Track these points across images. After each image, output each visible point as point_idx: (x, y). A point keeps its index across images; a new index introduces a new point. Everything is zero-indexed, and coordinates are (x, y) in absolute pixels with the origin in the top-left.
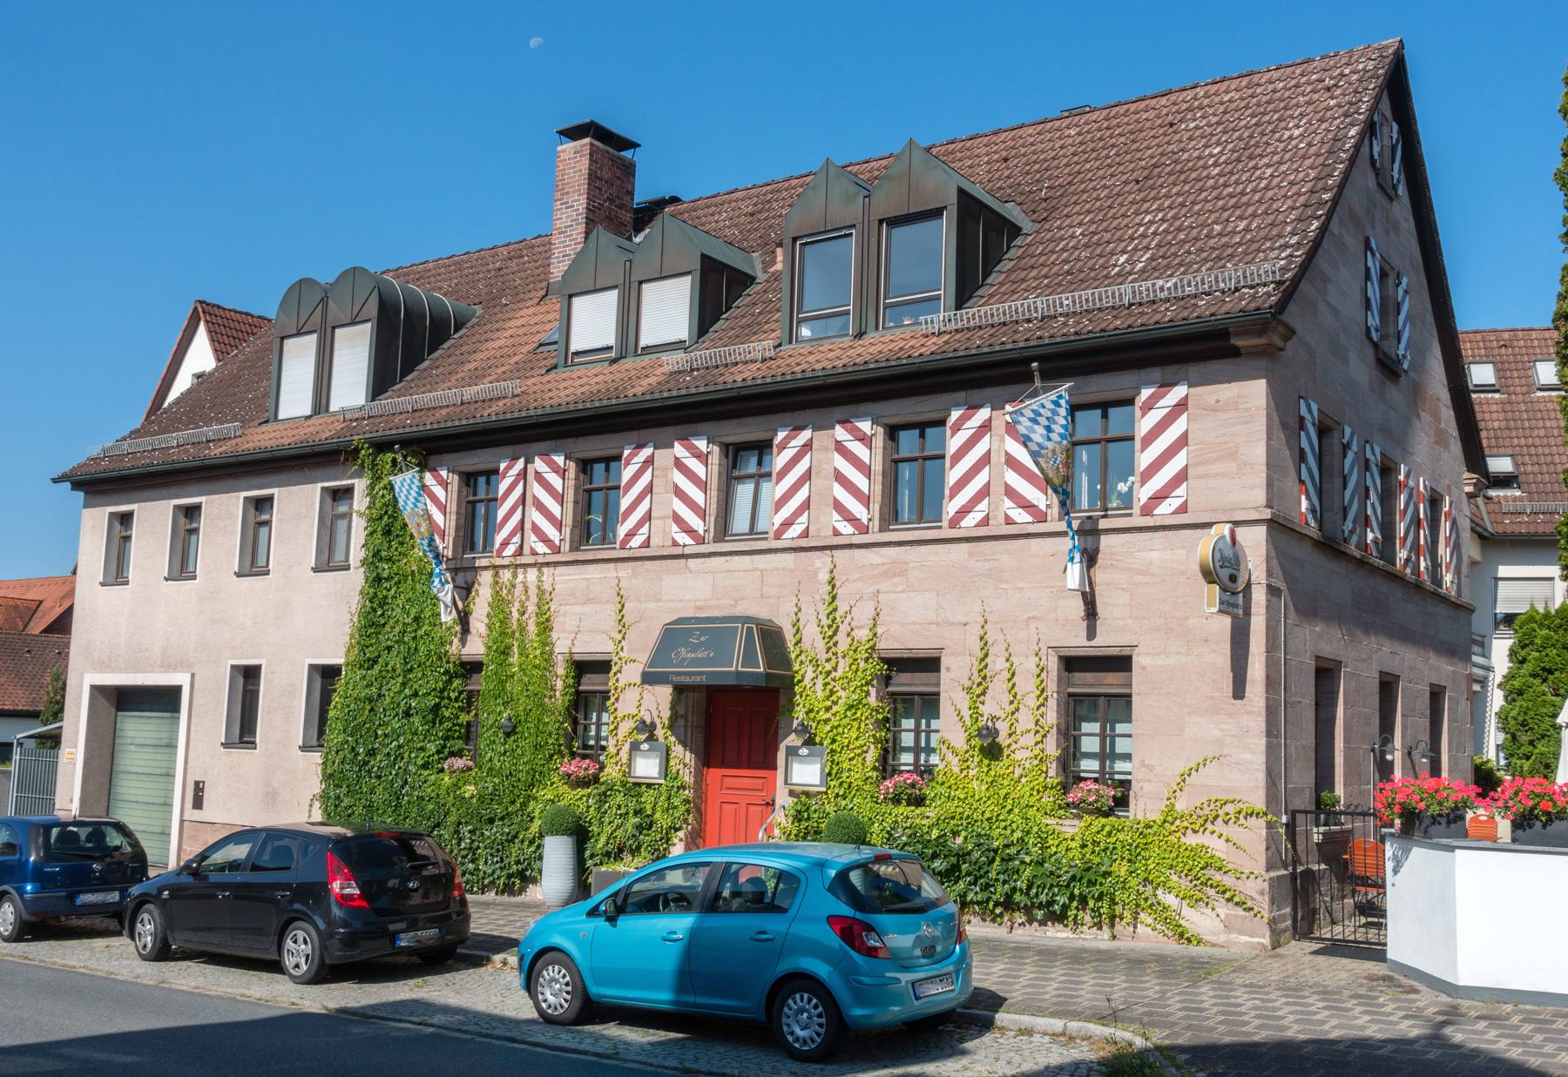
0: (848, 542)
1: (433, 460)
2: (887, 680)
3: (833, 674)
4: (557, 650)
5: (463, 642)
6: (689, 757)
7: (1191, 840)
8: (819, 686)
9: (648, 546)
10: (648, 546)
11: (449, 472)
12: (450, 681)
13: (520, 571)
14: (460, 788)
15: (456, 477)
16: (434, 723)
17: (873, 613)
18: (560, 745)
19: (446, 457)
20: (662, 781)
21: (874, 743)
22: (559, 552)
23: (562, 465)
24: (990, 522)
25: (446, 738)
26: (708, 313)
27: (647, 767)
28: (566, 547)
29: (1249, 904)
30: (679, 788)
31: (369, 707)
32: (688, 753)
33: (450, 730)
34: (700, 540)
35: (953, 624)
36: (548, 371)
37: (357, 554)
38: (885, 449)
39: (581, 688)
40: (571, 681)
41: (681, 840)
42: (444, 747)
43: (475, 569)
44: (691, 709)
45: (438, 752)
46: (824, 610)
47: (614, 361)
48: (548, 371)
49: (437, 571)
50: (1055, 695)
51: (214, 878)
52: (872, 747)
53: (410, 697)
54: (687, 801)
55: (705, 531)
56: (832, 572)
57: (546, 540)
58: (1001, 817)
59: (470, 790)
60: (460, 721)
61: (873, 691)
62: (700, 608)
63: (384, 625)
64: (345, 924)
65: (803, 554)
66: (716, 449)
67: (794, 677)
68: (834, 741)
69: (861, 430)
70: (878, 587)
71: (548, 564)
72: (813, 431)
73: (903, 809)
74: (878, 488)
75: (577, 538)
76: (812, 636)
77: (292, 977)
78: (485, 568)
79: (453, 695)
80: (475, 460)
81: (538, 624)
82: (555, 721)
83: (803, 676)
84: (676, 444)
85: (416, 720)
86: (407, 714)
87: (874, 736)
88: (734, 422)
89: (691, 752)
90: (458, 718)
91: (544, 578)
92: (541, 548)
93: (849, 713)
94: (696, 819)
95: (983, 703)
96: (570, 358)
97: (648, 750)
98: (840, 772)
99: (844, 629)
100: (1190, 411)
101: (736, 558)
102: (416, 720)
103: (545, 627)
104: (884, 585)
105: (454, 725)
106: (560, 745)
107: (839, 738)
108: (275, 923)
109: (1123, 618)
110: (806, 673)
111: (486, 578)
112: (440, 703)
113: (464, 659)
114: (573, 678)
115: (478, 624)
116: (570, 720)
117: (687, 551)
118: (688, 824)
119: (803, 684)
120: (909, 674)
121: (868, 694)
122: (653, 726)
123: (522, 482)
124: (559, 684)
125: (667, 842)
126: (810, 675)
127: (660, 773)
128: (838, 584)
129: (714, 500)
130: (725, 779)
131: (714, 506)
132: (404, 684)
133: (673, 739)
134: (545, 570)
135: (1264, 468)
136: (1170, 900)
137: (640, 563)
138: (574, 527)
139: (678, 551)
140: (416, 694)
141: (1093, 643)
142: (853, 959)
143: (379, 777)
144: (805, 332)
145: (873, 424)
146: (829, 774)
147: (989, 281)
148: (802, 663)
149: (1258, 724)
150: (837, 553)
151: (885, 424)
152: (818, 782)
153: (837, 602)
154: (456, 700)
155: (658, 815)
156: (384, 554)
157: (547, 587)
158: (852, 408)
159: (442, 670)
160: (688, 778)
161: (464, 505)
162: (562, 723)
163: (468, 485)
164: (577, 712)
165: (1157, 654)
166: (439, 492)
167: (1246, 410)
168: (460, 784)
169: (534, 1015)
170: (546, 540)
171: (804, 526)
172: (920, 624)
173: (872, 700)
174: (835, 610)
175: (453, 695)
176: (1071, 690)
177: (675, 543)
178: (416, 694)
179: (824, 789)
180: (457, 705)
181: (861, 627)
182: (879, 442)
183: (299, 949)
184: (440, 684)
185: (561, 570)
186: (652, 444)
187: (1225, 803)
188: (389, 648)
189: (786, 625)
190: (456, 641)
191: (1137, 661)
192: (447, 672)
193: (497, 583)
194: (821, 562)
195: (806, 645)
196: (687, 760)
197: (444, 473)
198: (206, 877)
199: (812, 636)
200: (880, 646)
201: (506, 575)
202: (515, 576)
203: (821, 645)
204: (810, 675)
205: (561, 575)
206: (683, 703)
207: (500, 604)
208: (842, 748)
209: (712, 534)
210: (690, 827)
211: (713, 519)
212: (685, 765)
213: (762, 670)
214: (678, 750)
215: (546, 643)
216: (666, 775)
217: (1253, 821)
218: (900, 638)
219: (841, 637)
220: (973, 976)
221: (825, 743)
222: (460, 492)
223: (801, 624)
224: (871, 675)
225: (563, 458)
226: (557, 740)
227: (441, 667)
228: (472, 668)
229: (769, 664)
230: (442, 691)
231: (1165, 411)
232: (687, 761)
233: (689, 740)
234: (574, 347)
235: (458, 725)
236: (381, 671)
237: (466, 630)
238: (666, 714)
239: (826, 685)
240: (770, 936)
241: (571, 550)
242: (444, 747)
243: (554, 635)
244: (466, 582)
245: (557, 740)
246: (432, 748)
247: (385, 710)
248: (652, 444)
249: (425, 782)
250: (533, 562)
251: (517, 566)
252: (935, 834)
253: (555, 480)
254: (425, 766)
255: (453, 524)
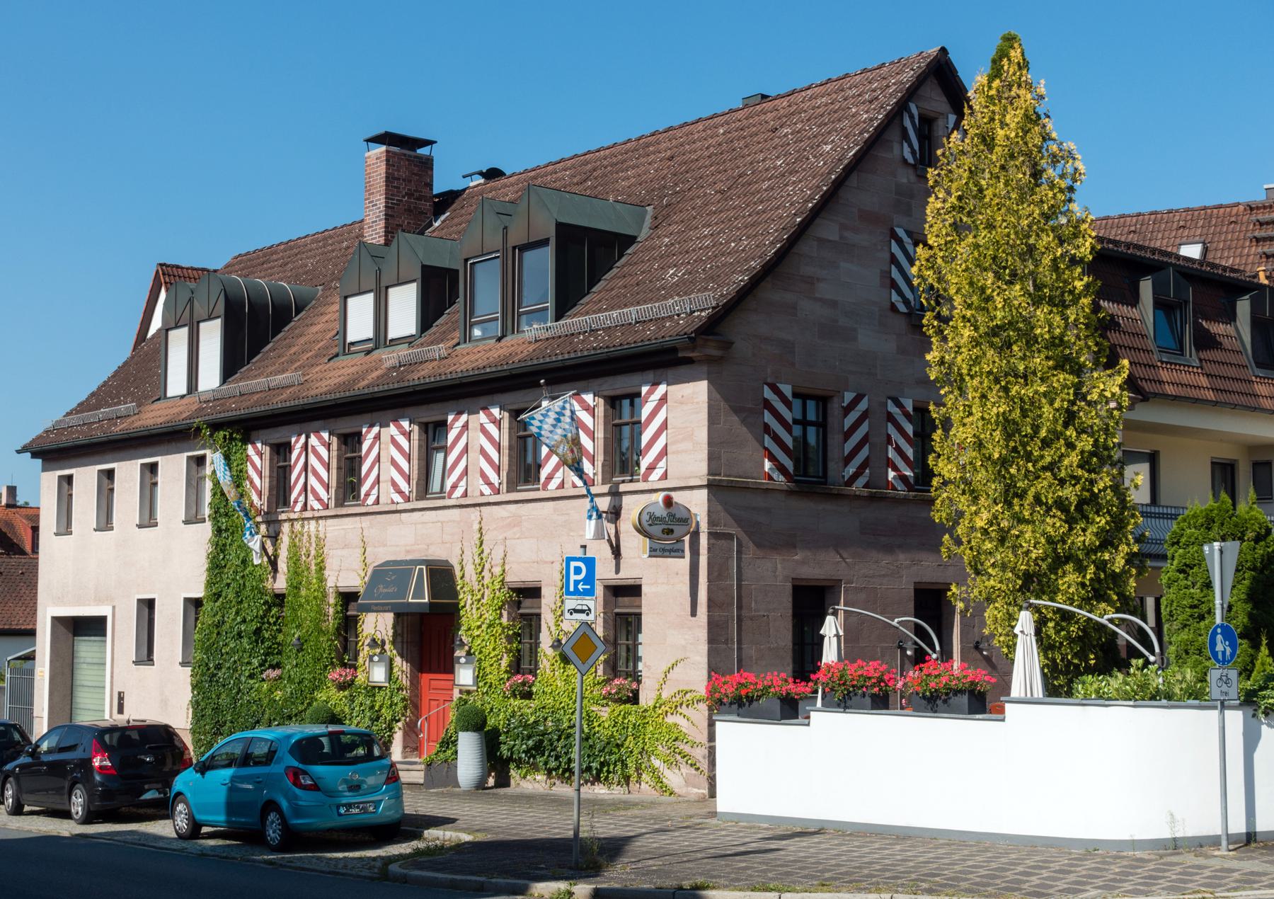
0: (486, 501)
1: (254, 434)
2: (519, 605)
3: (482, 601)
4: (329, 585)
5: (274, 578)
6: (406, 667)
7: (670, 720)
8: (474, 611)
9: (378, 504)
10: (378, 504)
11: (262, 444)
12: (269, 610)
13: (306, 522)
14: (273, 693)
15: (268, 448)
16: (258, 643)
17: (503, 555)
18: (332, 658)
19: (261, 432)
20: (387, 685)
21: (506, 653)
22: (328, 508)
23: (327, 440)
24: (565, 486)
25: (267, 654)
26: (429, 314)
27: (378, 674)
28: (332, 504)
29: (698, 765)
30: (398, 689)
31: (216, 631)
32: (404, 663)
33: (270, 647)
34: (408, 500)
35: (546, 562)
36: (329, 360)
37: (207, 511)
38: (605, 416)
39: (349, 613)
40: (339, 608)
41: (400, 729)
42: (265, 661)
43: (280, 522)
44: (405, 629)
45: (261, 665)
46: (476, 551)
47: (368, 352)
48: (329, 360)
49: (248, 525)
50: (602, 615)
51: (45, 759)
52: (505, 655)
53: (240, 623)
54: (404, 699)
55: (410, 492)
56: (480, 523)
57: (319, 500)
58: (570, 707)
59: (278, 695)
60: (278, 640)
61: (505, 613)
62: (408, 552)
63: (225, 566)
64: (102, 784)
65: (464, 510)
66: (416, 428)
67: (459, 603)
68: (481, 652)
69: (586, 402)
70: (505, 535)
71: (321, 518)
72: (469, 415)
73: (517, 702)
74: (506, 459)
75: (341, 496)
76: (470, 571)
77: (76, 820)
78: (285, 521)
79: (272, 620)
80: (278, 435)
81: (316, 565)
82: (326, 643)
83: (466, 602)
84: (391, 424)
85: (245, 640)
86: (240, 635)
87: (506, 648)
88: (424, 407)
89: (407, 662)
90: (276, 638)
91: (320, 529)
92: (317, 505)
93: (489, 630)
94: (412, 713)
95: (562, 621)
96: (347, 348)
97: (465, 663)
98: (485, 675)
99: (487, 566)
100: (668, 404)
101: (428, 513)
102: (245, 640)
103: (321, 569)
104: (509, 534)
105: (273, 644)
106: (332, 658)
107: (484, 650)
108: (67, 785)
109: (634, 558)
110: (465, 598)
111: (286, 528)
112: (261, 627)
113: (277, 592)
114: (341, 606)
115: (282, 565)
116: (341, 639)
117: (400, 507)
118: (406, 717)
119: (464, 609)
120: (530, 600)
121: (501, 615)
122: (383, 642)
123: (304, 453)
124: (331, 611)
125: (390, 731)
126: (469, 602)
127: (385, 679)
128: (484, 533)
129: (416, 467)
130: (432, 682)
131: (416, 472)
132: (237, 613)
133: (395, 652)
134: (320, 522)
135: (706, 446)
136: (656, 763)
137: (374, 516)
138: (338, 487)
139: (393, 508)
140: (244, 621)
141: (620, 576)
142: (294, 792)
143: (224, 686)
144: (477, 332)
145: (595, 396)
146: (478, 677)
147: (593, 290)
148: (464, 593)
149: (702, 634)
150: (483, 509)
151: (338, 434)
152: (471, 683)
153: (483, 546)
154: (275, 624)
155: (383, 710)
156: (222, 510)
157: (321, 535)
158: (489, 398)
159: (262, 602)
160: (405, 682)
161: (275, 470)
162: (333, 641)
163: (278, 453)
164: (347, 634)
165: (652, 584)
166: (256, 459)
167: (697, 403)
168: (273, 690)
169: (176, 836)
170: (319, 500)
171: (464, 488)
172: (529, 563)
173: (505, 621)
174: (482, 552)
175: (272, 620)
176: (617, 610)
177: (393, 502)
178: (244, 621)
179: (475, 688)
180: (275, 628)
181: (497, 565)
182: (600, 411)
183: (78, 804)
184: (261, 612)
185: (330, 521)
186: (378, 424)
187: (687, 693)
188: (228, 585)
189: (455, 562)
190: (271, 580)
191: (644, 589)
192: (266, 603)
193: (293, 532)
194: (474, 514)
195: (467, 579)
196: (404, 669)
197: (259, 445)
198: (39, 758)
199: (470, 571)
200: (507, 579)
201: (298, 526)
202: (303, 526)
203: (474, 577)
204: (469, 602)
205: (329, 526)
206: (400, 624)
207: (294, 546)
208: (485, 657)
209: (414, 494)
210: (408, 719)
211: (415, 482)
212: (403, 672)
213: (426, 600)
214: (398, 660)
215: (321, 580)
216: (390, 679)
217: (701, 704)
218: (519, 574)
219: (486, 573)
220: (405, 804)
221: (477, 653)
222: (271, 460)
223: (464, 563)
224: (502, 601)
225: (327, 434)
226: (330, 654)
227: (261, 599)
228: (280, 598)
229: (433, 594)
230: (262, 618)
231: (459, 429)
232: (404, 669)
233: (405, 652)
234: (350, 339)
235: (277, 643)
236: (223, 603)
237: (275, 569)
238: (391, 632)
239: (478, 609)
240: (261, 779)
241: (336, 506)
242: (265, 661)
243: (326, 573)
244: (275, 531)
245: (330, 654)
246: (255, 662)
247: (226, 633)
248: (378, 424)
249: (252, 688)
250: (311, 516)
251: (303, 519)
252: (532, 719)
253: (323, 452)
254: (251, 676)
255: (267, 485)
